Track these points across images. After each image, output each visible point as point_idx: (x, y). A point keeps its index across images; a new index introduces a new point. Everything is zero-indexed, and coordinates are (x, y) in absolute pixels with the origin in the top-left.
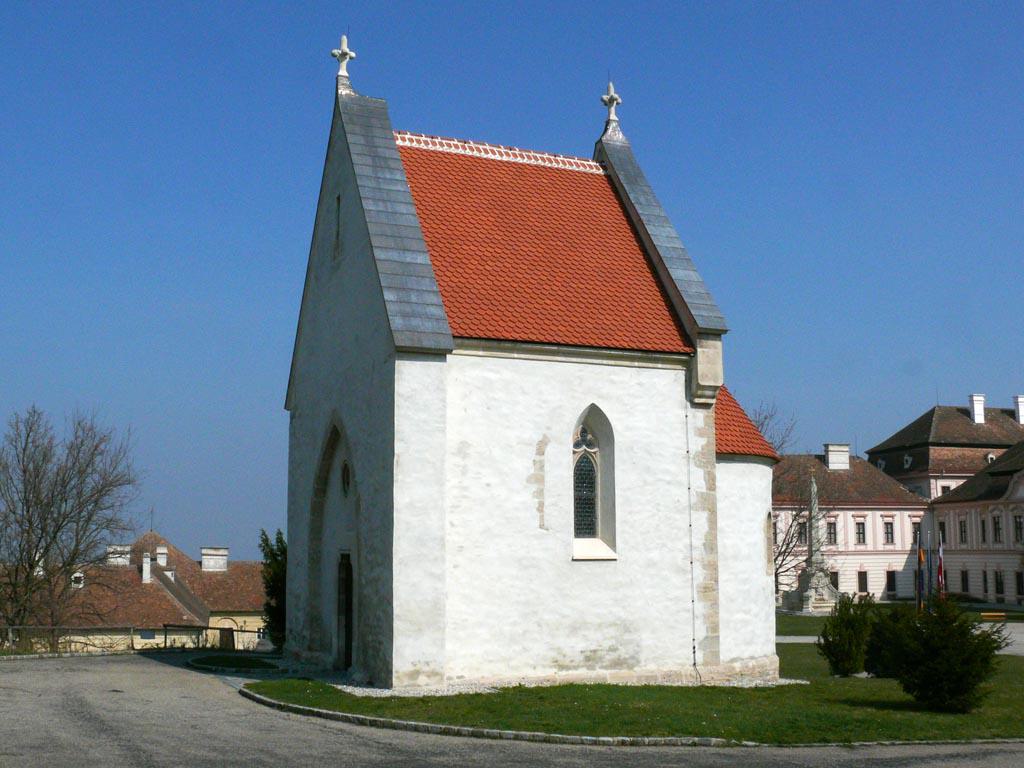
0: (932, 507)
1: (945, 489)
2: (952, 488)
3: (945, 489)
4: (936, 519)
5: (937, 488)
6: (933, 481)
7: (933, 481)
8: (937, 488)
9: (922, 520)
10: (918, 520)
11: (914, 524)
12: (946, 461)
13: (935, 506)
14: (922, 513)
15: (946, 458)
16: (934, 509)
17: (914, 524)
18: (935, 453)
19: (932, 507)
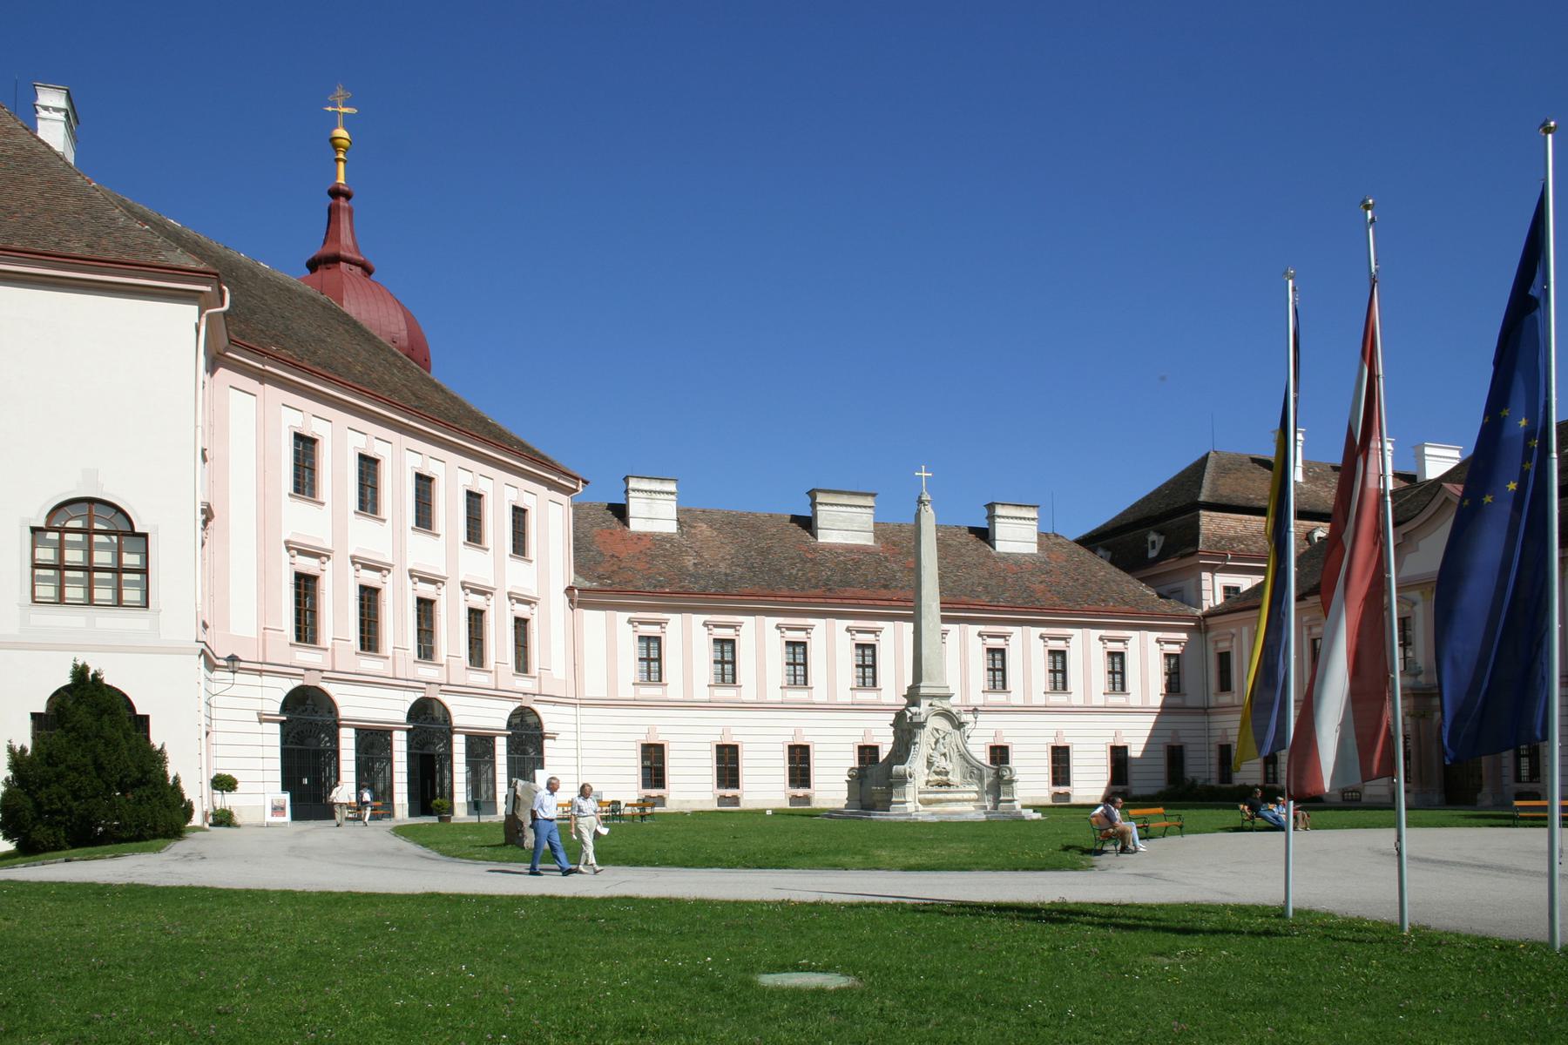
0: (1202, 626)
1: (1229, 591)
2: (1244, 588)
3: (1229, 591)
4: (1211, 647)
5: (1213, 589)
6: (1206, 576)
7: (1206, 576)
8: (1213, 589)
9: (1182, 651)
10: (1176, 649)
11: (1168, 656)
12: (1232, 539)
13: (1210, 621)
14: (1183, 636)
15: (1232, 533)
16: (1207, 629)
17: (1168, 656)
18: (1210, 523)
19: (1202, 626)
